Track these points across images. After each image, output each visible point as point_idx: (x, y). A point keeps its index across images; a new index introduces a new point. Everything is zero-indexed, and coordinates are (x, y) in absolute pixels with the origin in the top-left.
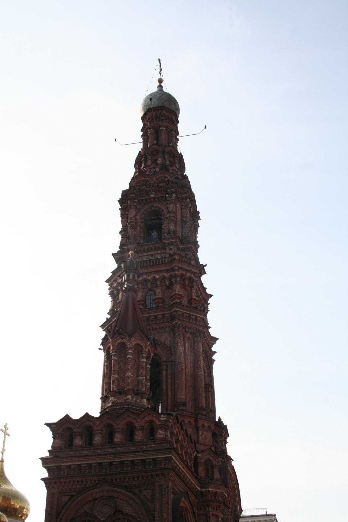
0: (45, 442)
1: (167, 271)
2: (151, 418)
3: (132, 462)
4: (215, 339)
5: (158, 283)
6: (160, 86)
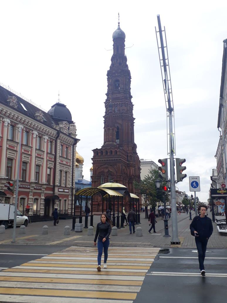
0: (92, 154)
1: (121, 101)
2: (116, 149)
3: (112, 160)
4: (134, 119)
5: (118, 105)
6: (119, 26)
